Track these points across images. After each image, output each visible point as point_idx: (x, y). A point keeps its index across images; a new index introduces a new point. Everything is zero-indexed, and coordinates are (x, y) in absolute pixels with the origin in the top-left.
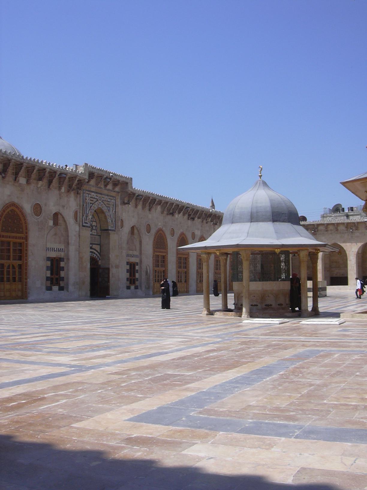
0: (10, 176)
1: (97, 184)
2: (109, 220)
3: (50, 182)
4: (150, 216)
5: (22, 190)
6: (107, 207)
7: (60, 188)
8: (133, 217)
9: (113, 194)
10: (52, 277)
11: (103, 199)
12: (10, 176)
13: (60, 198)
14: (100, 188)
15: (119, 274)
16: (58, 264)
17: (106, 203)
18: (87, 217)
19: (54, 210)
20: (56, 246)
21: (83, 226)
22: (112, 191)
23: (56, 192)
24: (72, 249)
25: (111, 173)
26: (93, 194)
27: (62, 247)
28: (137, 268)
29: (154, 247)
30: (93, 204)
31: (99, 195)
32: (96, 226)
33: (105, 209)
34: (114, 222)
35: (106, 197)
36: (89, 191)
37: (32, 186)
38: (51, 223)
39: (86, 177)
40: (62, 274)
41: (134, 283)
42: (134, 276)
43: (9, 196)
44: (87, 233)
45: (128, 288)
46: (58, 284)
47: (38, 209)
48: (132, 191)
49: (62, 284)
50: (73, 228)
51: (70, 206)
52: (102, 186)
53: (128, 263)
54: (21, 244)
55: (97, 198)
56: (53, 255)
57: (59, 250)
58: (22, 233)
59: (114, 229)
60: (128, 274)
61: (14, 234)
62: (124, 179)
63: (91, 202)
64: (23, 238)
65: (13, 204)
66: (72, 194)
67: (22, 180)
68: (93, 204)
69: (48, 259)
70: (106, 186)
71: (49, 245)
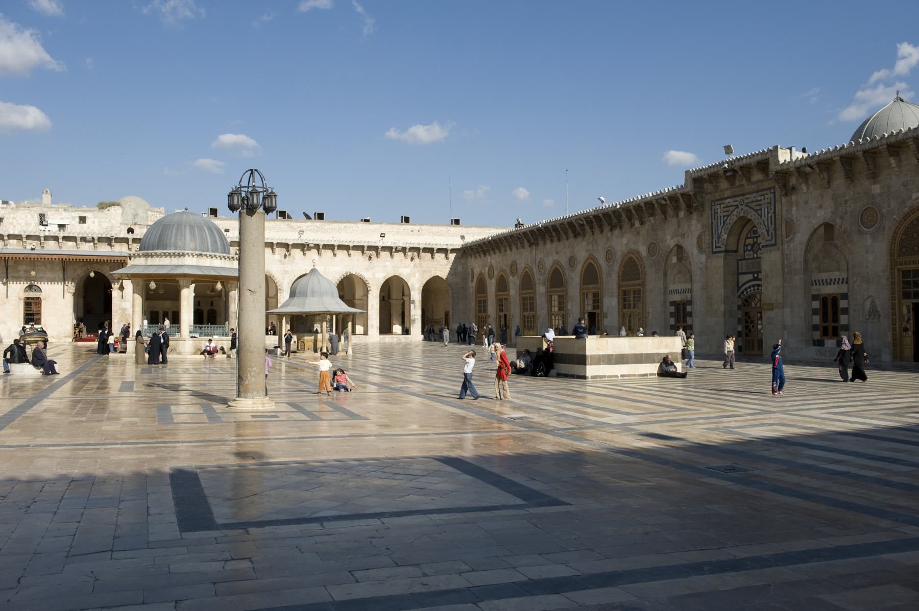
0: (626, 226)
1: (733, 184)
2: (762, 230)
3: (664, 213)
4: (876, 189)
5: (638, 233)
6: (756, 211)
7: (677, 216)
8: (821, 207)
9: (766, 185)
11: (746, 201)
12: (626, 226)
13: (679, 226)
14: (741, 186)
15: (786, 318)
16: (685, 309)
17: (753, 205)
18: (718, 238)
19: (671, 242)
20: (679, 287)
21: (714, 253)
22: (763, 181)
23: (675, 220)
24: (697, 287)
25: (723, 163)
26: (728, 200)
27: (689, 286)
28: (843, 304)
29: (892, 255)
30: (728, 216)
31: (738, 199)
33: (752, 215)
34: (772, 231)
35: (755, 195)
36: (720, 199)
37: (647, 226)
38: (674, 260)
39: (690, 189)
43: (626, 245)
44: (718, 261)
45: (819, 343)
47: (652, 249)
48: (778, 168)
50: (697, 258)
51: (691, 232)
52: (744, 182)
54: (639, 291)
55: (736, 203)
56: (677, 298)
57: (684, 291)
58: (639, 279)
59: (773, 242)
61: (632, 282)
62: (756, 158)
63: (725, 214)
64: (639, 285)
65: (631, 252)
66: (695, 215)
67: (637, 224)
68: (728, 216)
70: (749, 180)
71: (672, 287)
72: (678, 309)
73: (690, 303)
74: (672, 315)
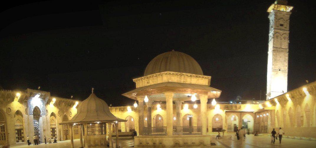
10: (19, 137)
16: (20, 131)
32: (36, 114)
40: (23, 135)
41: (55, 136)
42: (54, 133)
46: (21, 139)
49: (23, 139)
53: (51, 128)
56: (18, 128)
60: (52, 133)
69: (16, 130)
72: (18, 132)
73: (22, 129)
74: (16, 133)
